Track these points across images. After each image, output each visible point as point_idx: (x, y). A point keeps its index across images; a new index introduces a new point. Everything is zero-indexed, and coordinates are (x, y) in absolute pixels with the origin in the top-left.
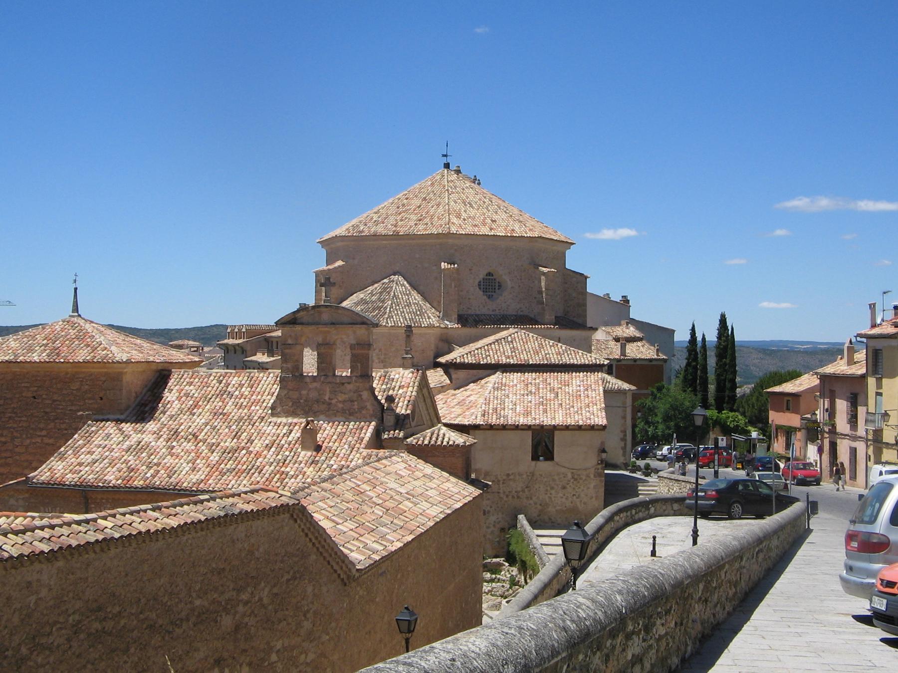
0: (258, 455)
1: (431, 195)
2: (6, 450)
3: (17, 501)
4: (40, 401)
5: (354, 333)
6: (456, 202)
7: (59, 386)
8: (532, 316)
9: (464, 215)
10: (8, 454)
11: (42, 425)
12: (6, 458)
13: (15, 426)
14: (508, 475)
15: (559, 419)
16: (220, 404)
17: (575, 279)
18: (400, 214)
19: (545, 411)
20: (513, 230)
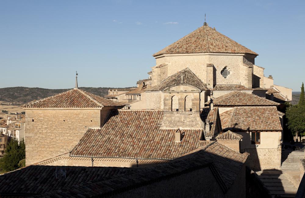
0: (158, 143)
1: (200, 36)
2: (53, 142)
3: (64, 162)
4: (67, 122)
5: (193, 94)
6: (210, 39)
7: (75, 116)
8: (243, 85)
9: (214, 44)
10: (54, 143)
11: (67, 132)
12: (53, 145)
13: (57, 132)
15: (262, 128)
16: (138, 123)
17: (258, 70)
18: (188, 44)
19: (256, 124)
20: (235, 50)
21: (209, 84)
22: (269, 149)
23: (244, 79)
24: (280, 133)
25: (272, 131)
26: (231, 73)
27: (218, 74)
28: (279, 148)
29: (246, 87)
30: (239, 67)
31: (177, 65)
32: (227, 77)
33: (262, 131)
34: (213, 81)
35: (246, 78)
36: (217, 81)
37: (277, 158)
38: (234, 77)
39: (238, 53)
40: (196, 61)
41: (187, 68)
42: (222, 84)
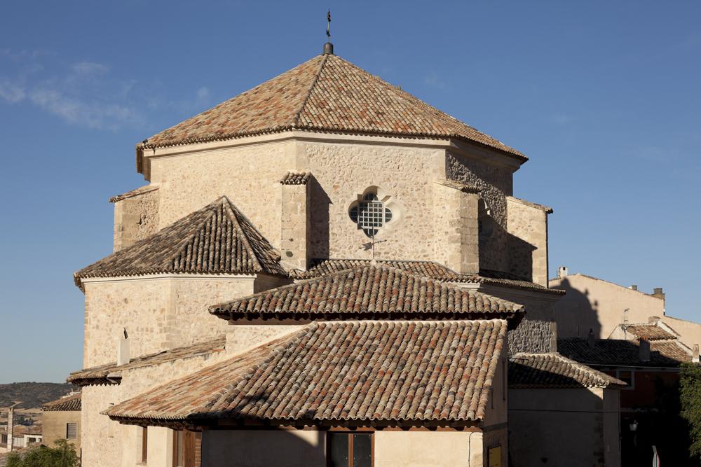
8: (442, 263)
9: (331, 104)
17: (525, 214)
21: (290, 254)
24: (477, 438)
25: (433, 429)
26: (396, 215)
27: (338, 218)
29: (453, 269)
30: (430, 191)
31: (190, 190)
32: (381, 231)
33: (382, 425)
34: (304, 240)
35: (455, 234)
36: (331, 246)
38: (407, 231)
39: (422, 136)
40: (252, 167)
42: (353, 258)
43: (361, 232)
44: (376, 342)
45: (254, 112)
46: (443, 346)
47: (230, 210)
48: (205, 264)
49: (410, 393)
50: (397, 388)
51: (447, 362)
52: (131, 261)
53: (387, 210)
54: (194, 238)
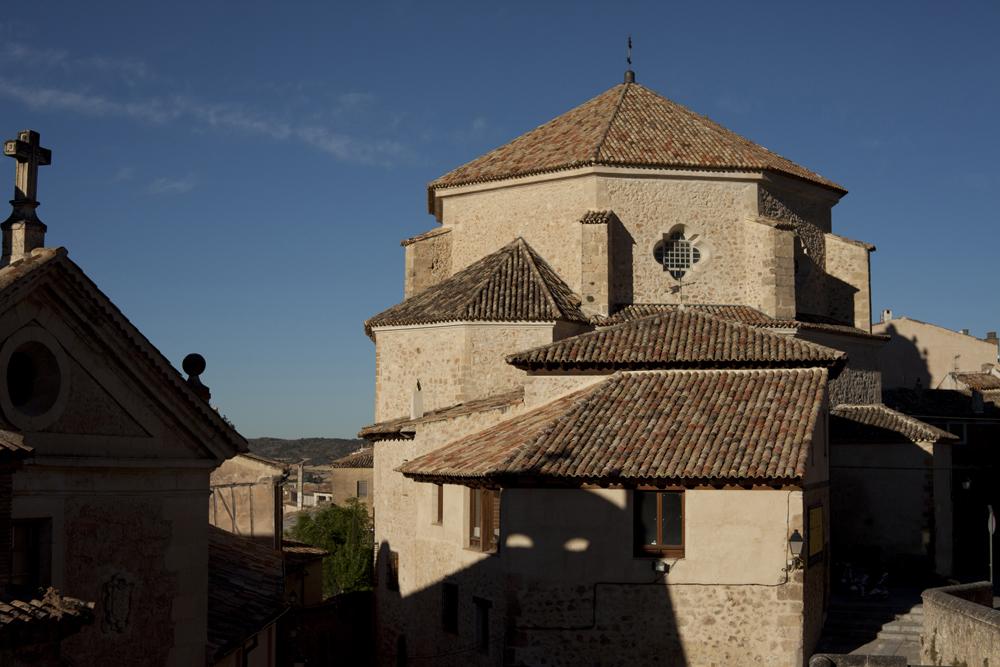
8: (756, 307)
14: (581, 590)
17: (845, 252)
21: (591, 299)
22: (735, 589)
23: (760, 279)
24: (796, 497)
25: (749, 487)
26: (705, 255)
27: (643, 259)
28: (787, 579)
29: (767, 313)
30: (741, 229)
31: (484, 232)
32: (689, 273)
33: (693, 483)
34: (606, 283)
35: (769, 275)
36: (635, 290)
37: (780, 640)
38: (717, 273)
39: (732, 169)
40: (549, 206)
41: (516, 240)
42: (659, 302)
43: (667, 274)
44: (685, 393)
45: (551, 147)
46: (758, 397)
47: (526, 252)
48: (501, 310)
49: (723, 448)
50: (708, 443)
51: (763, 414)
52: (423, 308)
53: (695, 250)
54: (489, 283)
